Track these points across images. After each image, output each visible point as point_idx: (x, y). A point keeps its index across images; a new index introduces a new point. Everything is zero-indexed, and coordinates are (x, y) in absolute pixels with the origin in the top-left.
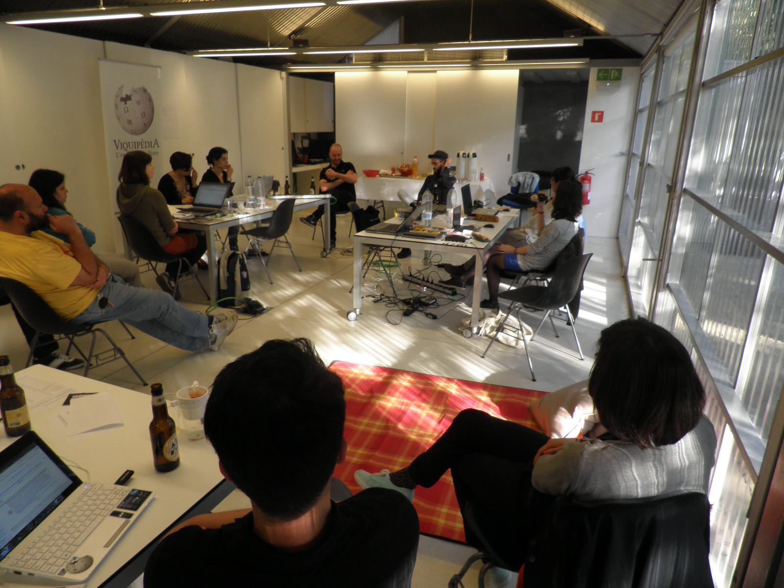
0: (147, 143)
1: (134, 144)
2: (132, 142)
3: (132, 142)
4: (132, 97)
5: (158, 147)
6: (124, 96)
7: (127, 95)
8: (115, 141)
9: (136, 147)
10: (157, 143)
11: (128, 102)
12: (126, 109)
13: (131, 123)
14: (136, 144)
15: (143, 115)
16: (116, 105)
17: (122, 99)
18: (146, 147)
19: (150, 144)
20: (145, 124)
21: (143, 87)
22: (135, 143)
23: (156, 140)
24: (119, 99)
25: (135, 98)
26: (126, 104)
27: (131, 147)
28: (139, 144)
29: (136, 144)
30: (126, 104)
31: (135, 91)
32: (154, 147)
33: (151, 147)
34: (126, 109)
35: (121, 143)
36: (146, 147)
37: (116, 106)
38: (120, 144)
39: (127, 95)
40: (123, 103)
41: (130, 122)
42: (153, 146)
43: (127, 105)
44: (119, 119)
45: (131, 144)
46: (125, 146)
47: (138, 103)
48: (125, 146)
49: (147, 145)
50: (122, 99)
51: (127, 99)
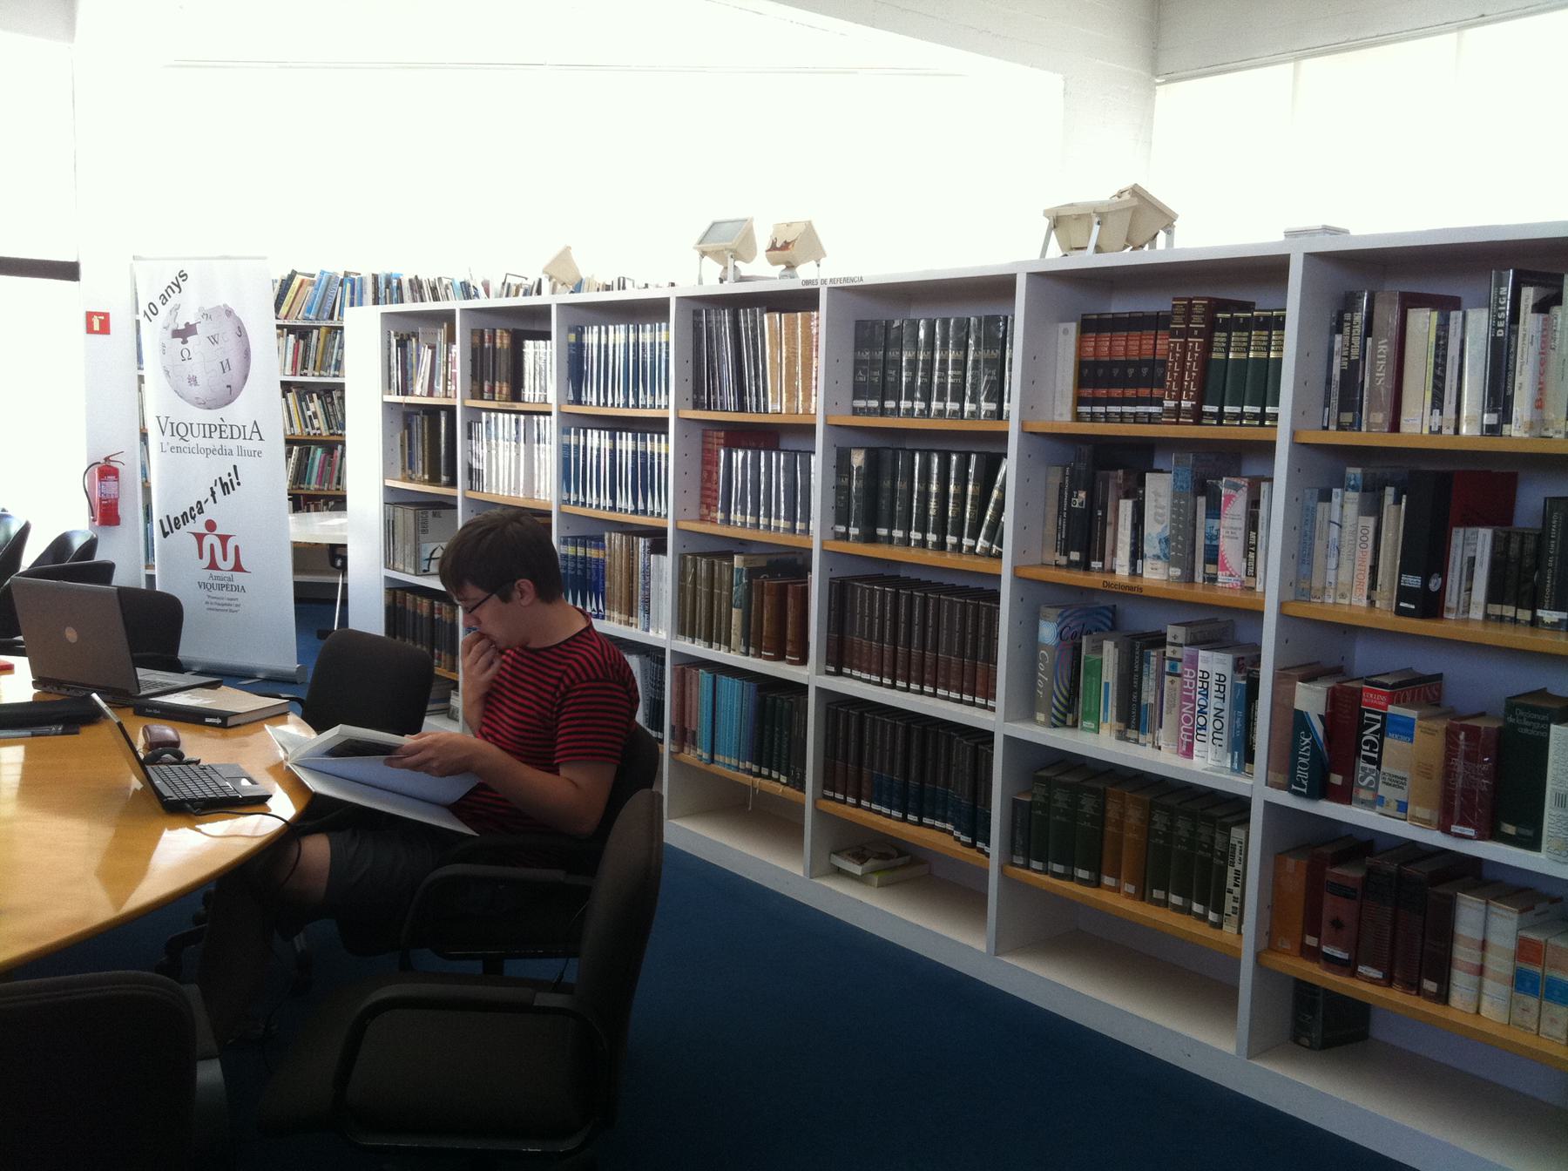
0: (235, 430)
1: (201, 426)
5: (261, 439)
6: (182, 327)
7: (187, 324)
8: (158, 417)
9: (208, 434)
10: (258, 432)
13: (196, 384)
14: (207, 427)
15: (225, 366)
17: (177, 334)
18: (232, 438)
20: (228, 386)
21: (229, 312)
22: (204, 425)
23: (255, 422)
27: (195, 434)
28: (213, 428)
29: (207, 427)
30: (185, 342)
31: (206, 316)
32: (250, 439)
33: (245, 439)
34: (185, 353)
35: (172, 424)
36: (232, 438)
38: (169, 425)
39: (187, 324)
41: (193, 380)
42: (248, 437)
45: (195, 427)
46: (182, 430)
47: (213, 340)
48: (182, 430)
49: (236, 434)
50: (177, 334)
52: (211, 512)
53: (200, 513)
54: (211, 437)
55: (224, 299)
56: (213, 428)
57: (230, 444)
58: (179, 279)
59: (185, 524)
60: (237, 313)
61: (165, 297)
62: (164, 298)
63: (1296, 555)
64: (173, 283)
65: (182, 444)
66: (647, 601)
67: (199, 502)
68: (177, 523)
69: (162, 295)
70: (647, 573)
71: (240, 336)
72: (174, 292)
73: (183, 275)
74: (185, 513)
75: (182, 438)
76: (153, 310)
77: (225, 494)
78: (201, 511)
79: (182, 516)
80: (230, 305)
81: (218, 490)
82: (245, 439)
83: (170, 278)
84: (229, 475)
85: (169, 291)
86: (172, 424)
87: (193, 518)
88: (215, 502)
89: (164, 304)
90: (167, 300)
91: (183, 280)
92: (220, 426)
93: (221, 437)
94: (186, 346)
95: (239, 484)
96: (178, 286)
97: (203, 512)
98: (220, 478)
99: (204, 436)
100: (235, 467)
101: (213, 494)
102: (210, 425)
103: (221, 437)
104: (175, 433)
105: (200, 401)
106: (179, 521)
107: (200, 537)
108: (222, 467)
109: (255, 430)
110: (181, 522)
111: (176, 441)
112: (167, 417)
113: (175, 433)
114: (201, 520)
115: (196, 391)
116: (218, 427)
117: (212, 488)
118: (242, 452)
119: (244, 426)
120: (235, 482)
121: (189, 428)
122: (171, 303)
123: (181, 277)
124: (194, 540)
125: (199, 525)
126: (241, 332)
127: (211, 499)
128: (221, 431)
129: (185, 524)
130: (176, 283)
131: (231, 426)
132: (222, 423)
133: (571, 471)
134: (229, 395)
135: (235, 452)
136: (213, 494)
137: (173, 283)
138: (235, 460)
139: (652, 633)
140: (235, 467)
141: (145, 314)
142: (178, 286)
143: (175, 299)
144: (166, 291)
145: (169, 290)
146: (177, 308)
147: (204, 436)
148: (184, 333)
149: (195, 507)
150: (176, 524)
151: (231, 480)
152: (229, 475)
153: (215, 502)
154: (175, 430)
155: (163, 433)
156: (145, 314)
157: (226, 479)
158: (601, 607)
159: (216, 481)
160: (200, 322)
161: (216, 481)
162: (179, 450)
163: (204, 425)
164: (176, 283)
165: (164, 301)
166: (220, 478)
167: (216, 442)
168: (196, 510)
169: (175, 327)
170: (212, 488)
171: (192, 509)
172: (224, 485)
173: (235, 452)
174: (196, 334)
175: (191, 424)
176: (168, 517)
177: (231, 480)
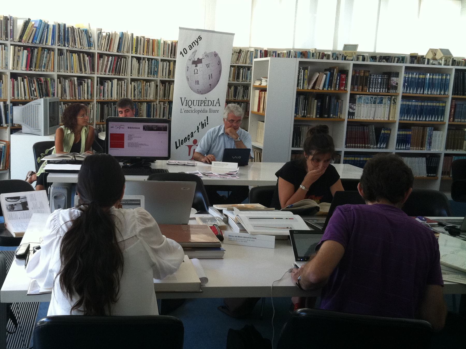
0: (210, 102)
1: (198, 101)
2: (197, 101)
3: (197, 101)
5: (220, 106)
6: (196, 60)
8: (181, 98)
9: (200, 105)
10: (219, 103)
12: (196, 71)
13: (198, 84)
14: (200, 102)
15: (210, 77)
16: (188, 67)
18: (208, 106)
19: (212, 103)
20: (210, 85)
21: (216, 55)
22: (199, 101)
24: (191, 61)
27: (195, 104)
28: (202, 101)
29: (200, 102)
30: (196, 66)
31: (207, 56)
32: (215, 106)
33: (213, 106)
34: (196, 71)
35: (187, 101)
36: (208, 106)
38: (185, 101)
41: (197, 82)
45: (195, 102)
47: (208, 66)
51: (199, 61)
52: (196, 136)
53: (191, 137)
54: (201, 106)
55: (214, 49)
56: (202, 101)
57: (207, 108)
58: (198, 40)
59: (185, 142)
60: (219, 55)
61: (191, 47)
62: (191, 47)
64: (195, 41)
65: (189, 109)
66: (430, 144)
67: (192, 133)
68: (182, 142)
69: (190, 45)
70: (431, 136)
71: (219, 65)
72: (195, 45)
73: (200, 38)
74: (186, 138)
75: (189, 107)
76: (185, 51)
77: (202, 128)
78: (192, 136)
79: (185, 139)
80: (217, 52)
81: (200, 127)
82: (213, 106)
83: (194, 38)
84: (205, 120)
85: (194, 44)
86: (187, 101)
87: (189, 139)
88: (198, 132)
89: (190, 49)
90: (192, 48)
91: (200, 40)
92: (205, 101)
93: (204, 105)
94: (196, 68)
95: (208, 124)
96: (197, 42)
97: (193, 136)
98: (202, 122)
99: (198, 106)
100: (207, 117)
101: (198, 128)
102: (201, 101)
103: (204, 105)
104: (187, 105)
105: (199, 91)
106: (183, 142)
107: (190, 147)
108: (202, 118)
109: (218, 102)
110: (184, 142)
111: (187, 108)
112: (185, 98)
113: (187, 105)
114: (192, 139)
115: (197, 87)
116: (204, 101)
117: (198, 126)
118: (211, 111)
119: (213, 101)
120: (206, 123)
121: (193, 102)
122: (193, 50)
123: (199, 38)
124: (188, 148)
125: (190, 142)
126: (219, 63)
127: (197, 131)
128: (205, 103)
129: (185, 142)
130: (197, 41)
131: (208, 101)
132: (206, 100)
133: (405, 111)
134: (211, 87)
135: (208, 111)
136: (198, 128)
137: (195, 41)
138: (208, 114)
139: (432, 150)
140: (207, 117)
141: (181, 53)
142: (197, 42)
144: (192, 44)
145: (194, 44)
147: (198, 106)
148: (197, 62)
149: (190, 135)
150: (182, 143)
151: (205, 123)
152: (205, 120)
153: (198, 132)
155: (182, 105)
156: (181, 53)
157: (203, 122)
158: (409, 146)
159: (200, 123)
160: (204, 58)
161: (200, 123)
162: (188, 111)
163: (199, 101)
164: (197, 41)
165: (191, 48)
166: (202, 122)
167: (202, 107)
168: (190, 136)
169: (193, 59)
170: (198, 126)
171: (189, 136)
172: (203, 125)
173: (208, 111)
174: (202, 63)
175: (194, 101)
176: (179, 140)
177: (205, 123)
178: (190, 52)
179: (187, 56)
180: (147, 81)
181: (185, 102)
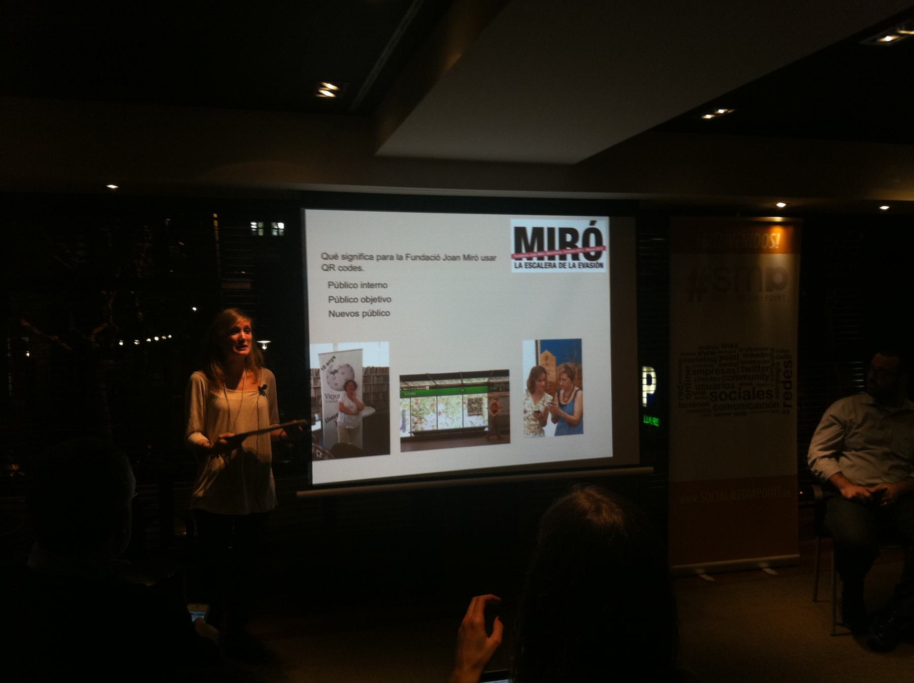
4: (339, 371)
6: (333, 371)
11: (336, 374)
21: (348, 366)
24: (329, 373)
25: (340, 371)
26: (334, 375)
30: (334, 375)
31: (341, 367)
37: (327, 377)
40: (332, 375)
41: (336, 384)
43: (335, 376)
44: (328, 383)
46: (333, 397)
47: (343, 374)
48: (333, 397)
51: (336, 371)
55: (346, 362)
62: (328, 364)
63: (645, 381)
73: (334, 357)
80: (349, 364)
111: (331, 400)
143: (331, 363)
146: (331, 367)
154: (330, 397)
162: (331, 402)
171: (334, 416)
178: (327, 367)
179: (326, 370)
180: (384, 384)
181: (329, 396)
